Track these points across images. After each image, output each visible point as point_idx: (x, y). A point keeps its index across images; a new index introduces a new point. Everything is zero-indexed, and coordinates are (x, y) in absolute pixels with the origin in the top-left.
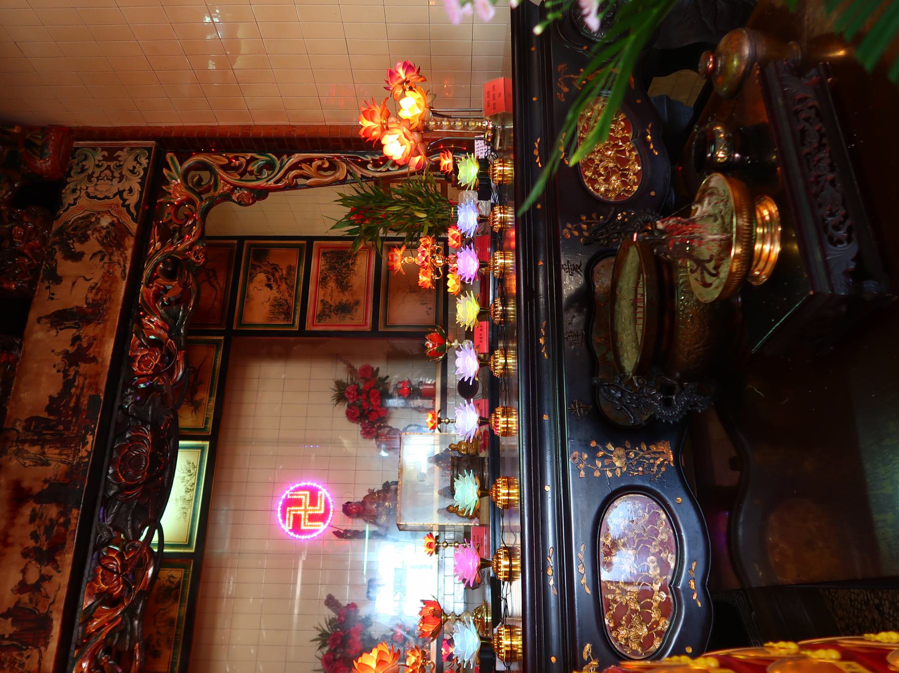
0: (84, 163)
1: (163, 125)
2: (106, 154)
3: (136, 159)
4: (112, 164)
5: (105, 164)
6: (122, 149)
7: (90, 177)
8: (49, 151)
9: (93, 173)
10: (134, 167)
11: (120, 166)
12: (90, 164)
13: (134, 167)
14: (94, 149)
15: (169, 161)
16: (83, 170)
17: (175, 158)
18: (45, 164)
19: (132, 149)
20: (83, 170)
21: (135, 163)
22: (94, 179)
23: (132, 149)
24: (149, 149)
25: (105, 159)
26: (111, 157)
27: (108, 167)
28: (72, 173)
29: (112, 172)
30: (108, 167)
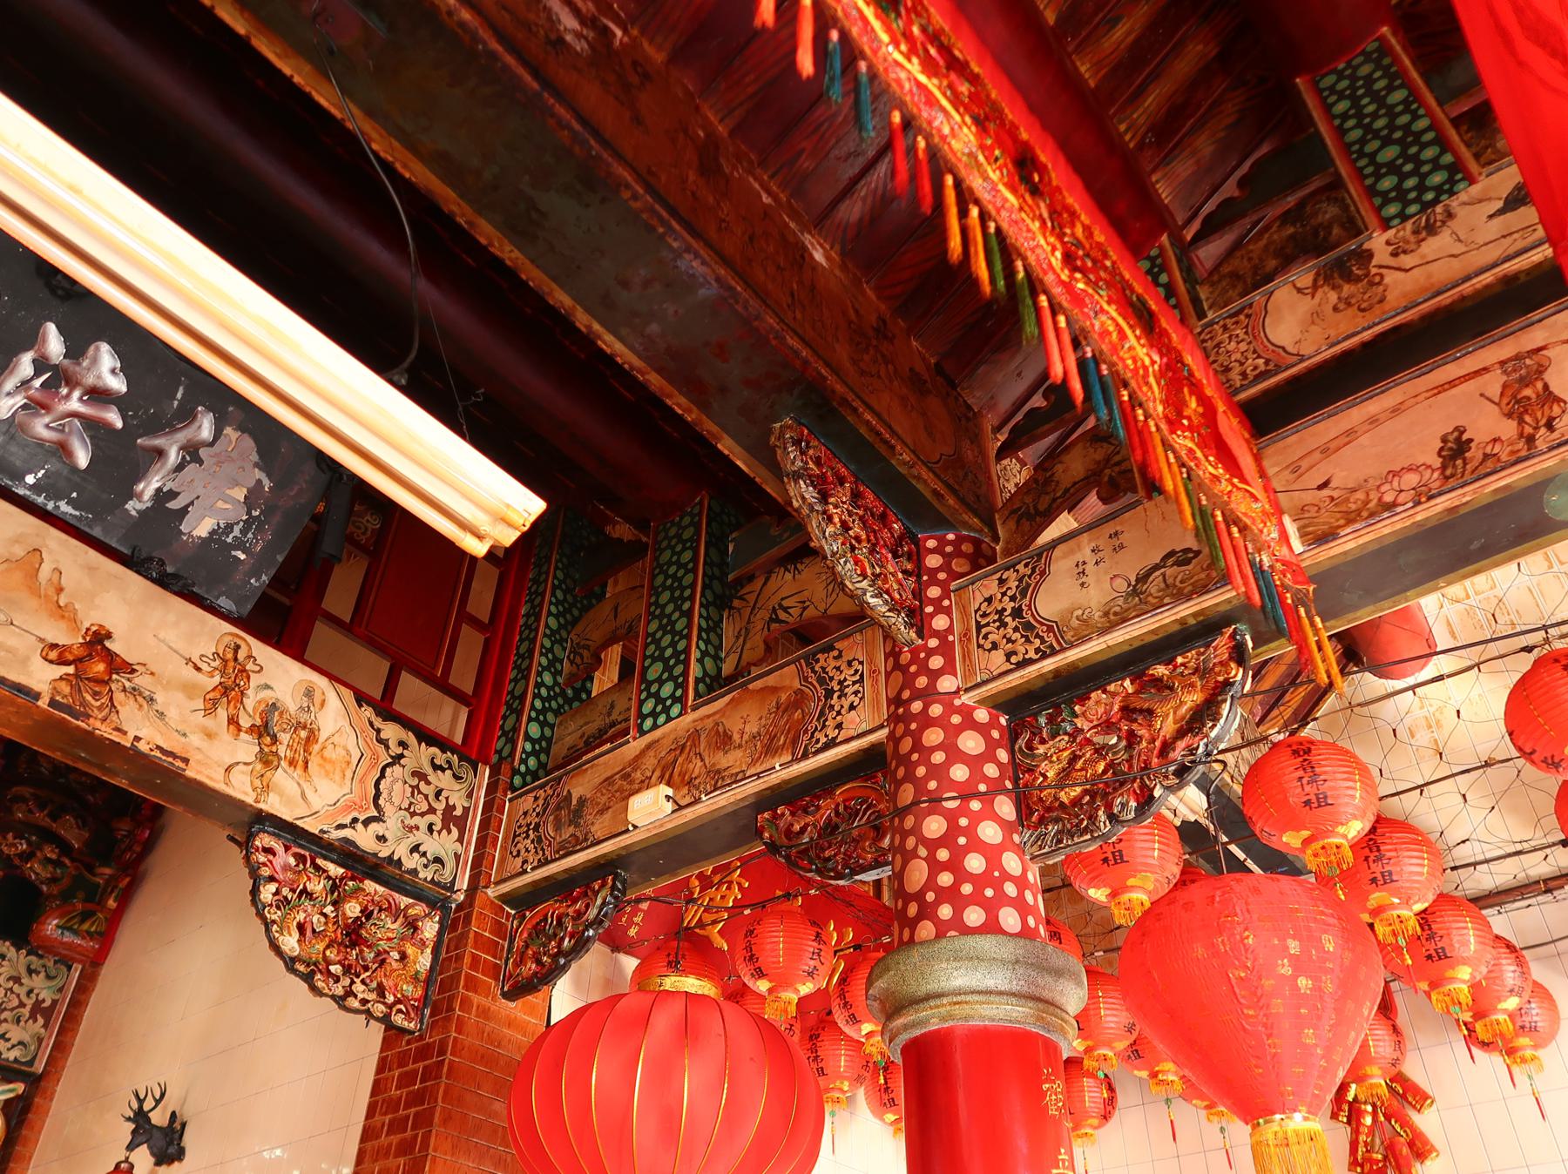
0: (42, 975)
1: (58, 1089)
2: (47, 1004)
3: (20, 1043)
4: (26, 1012)
5: (29, 1002)
6: (45, 1026)
7: (17, 980)
8: (68, 937)
9: (21, 984)
10: (8, 1040)
11: (18, 1021)
12: (38, 981)
13: (8, 1040)
14: (60, 990)
15: (11, 1086)
16: (30, 972)
17: (12, 1095)
18: (51, 926)
19: (40, 1040)
20: (30, 972)
21: (14, 1041)
22: (11, 984)
23: (40, 1040)
24: (31, 1063)
25: (38, 1003)
26: (37, 1009)
27: (22, 1005)
28: (33, 958)
29: (12, 1010)
30: (22, 1005)
